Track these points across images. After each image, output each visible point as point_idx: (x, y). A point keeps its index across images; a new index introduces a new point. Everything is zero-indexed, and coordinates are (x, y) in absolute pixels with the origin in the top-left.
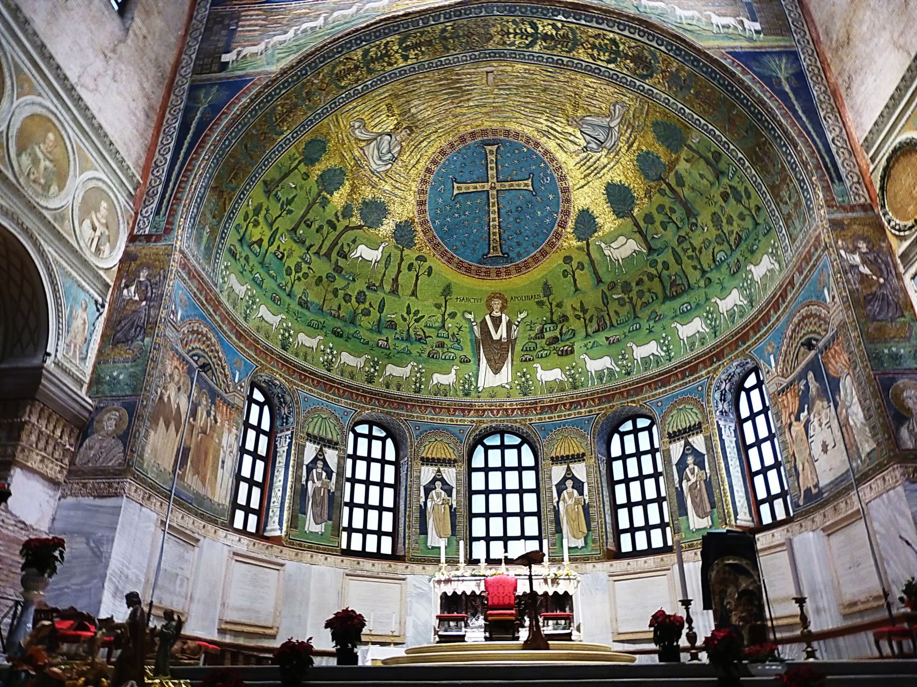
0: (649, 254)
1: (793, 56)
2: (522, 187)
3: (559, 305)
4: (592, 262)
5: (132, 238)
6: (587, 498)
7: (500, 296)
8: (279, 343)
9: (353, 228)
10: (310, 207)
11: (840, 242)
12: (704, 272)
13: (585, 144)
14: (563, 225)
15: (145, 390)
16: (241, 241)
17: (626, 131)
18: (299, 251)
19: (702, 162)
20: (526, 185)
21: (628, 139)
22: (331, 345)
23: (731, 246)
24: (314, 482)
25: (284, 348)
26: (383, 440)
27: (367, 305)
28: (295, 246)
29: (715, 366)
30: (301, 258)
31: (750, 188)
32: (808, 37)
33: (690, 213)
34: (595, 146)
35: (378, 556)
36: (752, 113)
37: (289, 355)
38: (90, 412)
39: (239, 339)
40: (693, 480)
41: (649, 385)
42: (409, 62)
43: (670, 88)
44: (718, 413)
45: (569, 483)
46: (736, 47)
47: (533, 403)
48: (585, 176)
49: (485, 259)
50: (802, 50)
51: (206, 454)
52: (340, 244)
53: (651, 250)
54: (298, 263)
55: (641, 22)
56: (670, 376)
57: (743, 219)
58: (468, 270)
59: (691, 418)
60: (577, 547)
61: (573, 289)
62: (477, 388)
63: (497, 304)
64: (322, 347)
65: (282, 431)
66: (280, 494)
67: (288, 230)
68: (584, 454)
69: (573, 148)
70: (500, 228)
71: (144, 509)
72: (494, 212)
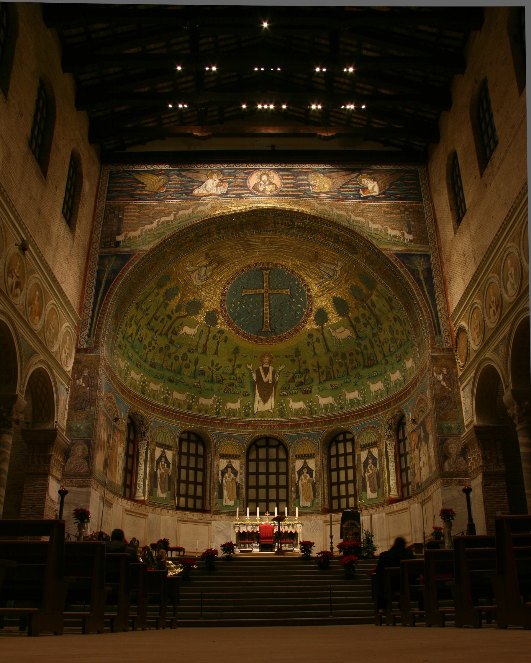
0: (357, 339)
1: (427, 257)
2: (284, 293)
3: (304, 362)
4: (324, 338)
5: (78, 351)
6: (314, 479)
7: (269, 355)
8: (140, 390)
9: (181, 317)
10: (158, 310)
11: (434, 368)
12: (385, 356)
13: (321, 275)
14: (308, 316)
15: (95, 435)
16: (123, 338)
17: (344, 274)
18: (150, 334)
19: (383, 300)
20: (287, 292)
21: (346, 277)
22: (167, 388)
23: (397, 346)
24: (160, 470)
25: (143, 393)
27: (188, 362)
28: (148, 332)
29: (386, 410)
30: (152, 339)
31: (405, 321)
32: (436, 246)
33: (378, 322)
34: (327, 277)
36: (405, 288)
37: (145, 397)
38: (69, 446)
39: (122, 393)
40: (371, 472)
41: (353, 416)
42: (221, 235)
43: (366, 262)
44: (386, 437)
45: (305, 471)
46: (398, 250)
47: (287, 422)
48: (321, 291)
49: (259, 332)
50: (432, 254)
51: (112, 460)
52: (173, 327)
53: (357, 336)
54: (150, 341)
56: (364, 412)
57: (403, 334)
58: (250, 338)
59: (373, 438)
60: (307, 507)
61: (313, 353)
62: (253, 411)
63: (266, 359)
64: (163, 390)
65: (142, 441)
66: (142, 477)
67: (145, 325)
68: (314, 454)
69: (314, 276)
70: (270, 314)
71: (97, 492)
72: (266, 306)
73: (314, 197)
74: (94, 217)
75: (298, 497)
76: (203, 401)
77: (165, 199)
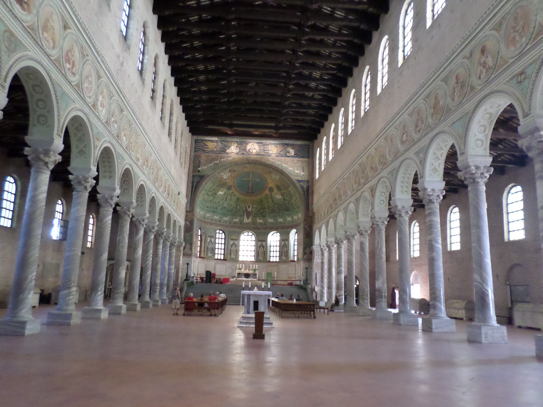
4: (272, 197)
5: (186, 211)
14: (266, 188)
26: (222, 233)
33: (291, 197)
35: (220, 259)
37: (205, 220)
45: (261, 246)
49: (248, 192)
53: (284, 199)
55: (282, 170)
60: (261, 260)
62: (243, 223)
73: (270, 156)
74: (190, 159)
75: (258, 256)
76: (225, 219)
77: (216, 153)
